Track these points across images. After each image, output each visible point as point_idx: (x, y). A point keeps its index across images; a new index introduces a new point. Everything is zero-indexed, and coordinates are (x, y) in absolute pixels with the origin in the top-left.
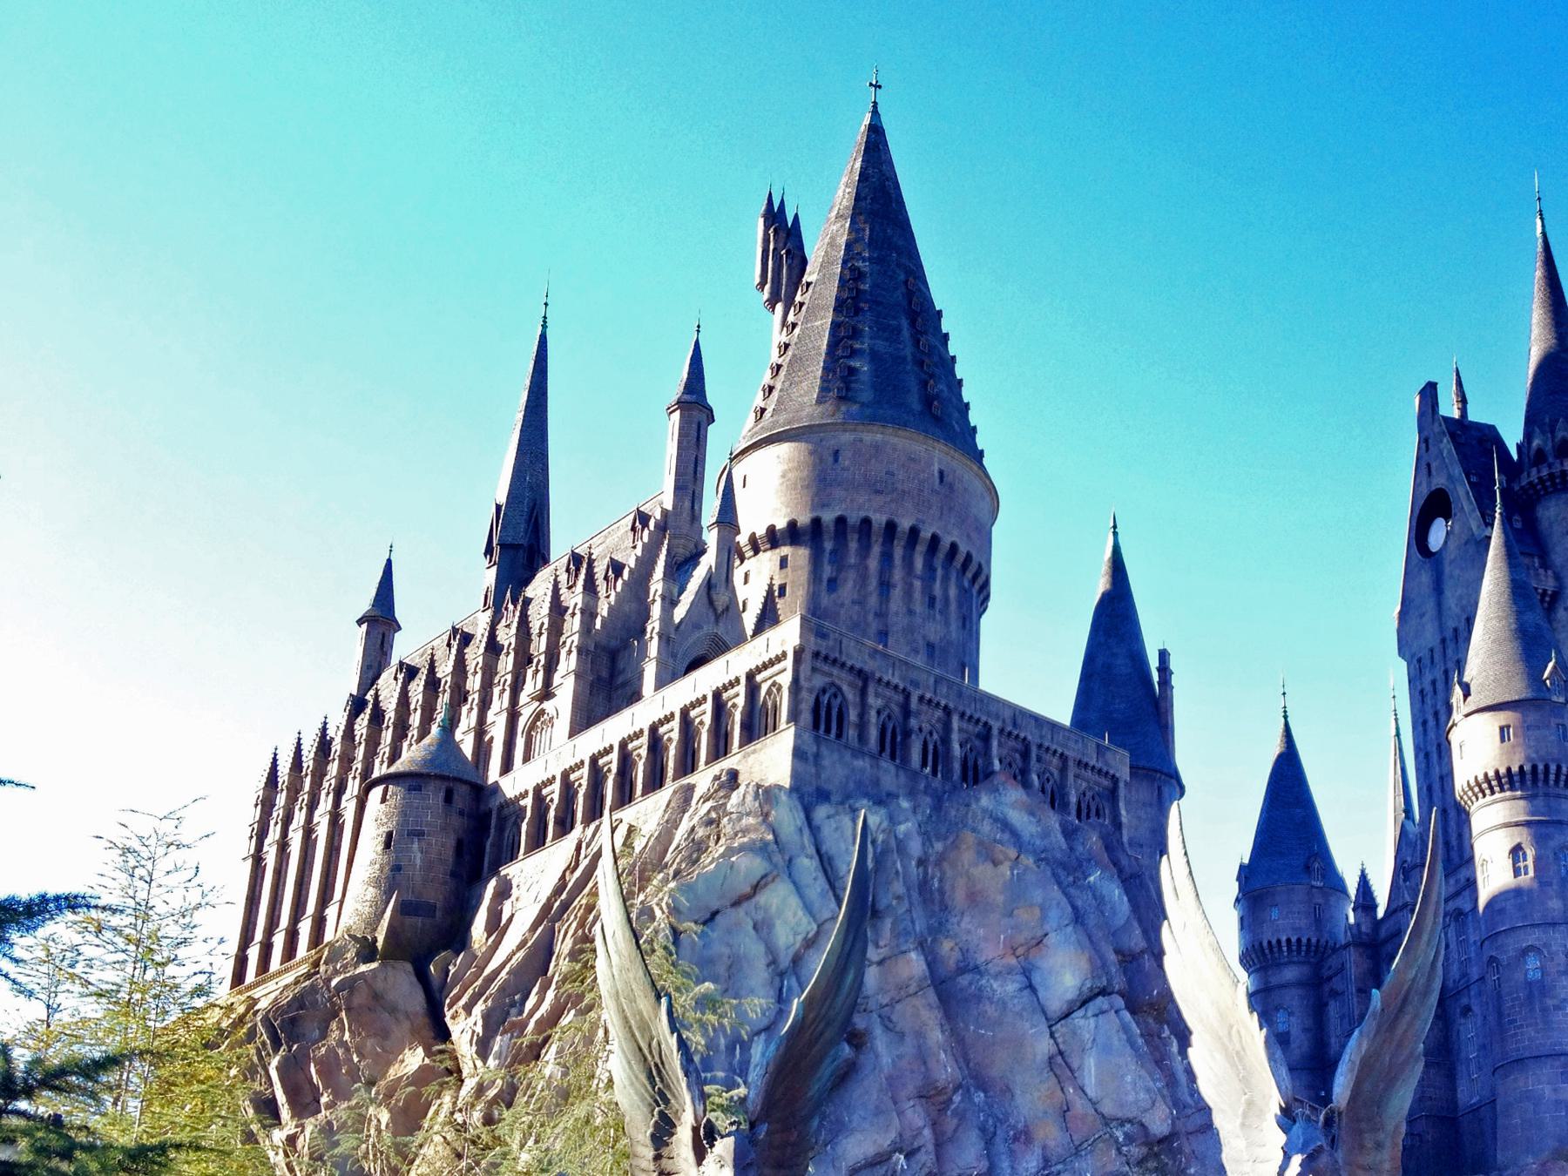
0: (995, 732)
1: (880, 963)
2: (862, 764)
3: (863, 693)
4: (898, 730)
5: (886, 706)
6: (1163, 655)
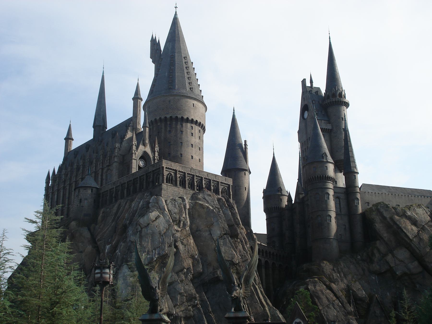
0: (203, 178)
1: (180, 231)
2: (176, 189)
3: (176, 174)
4: (183, 181)
5: (181, 176)
6: (245, 141)
